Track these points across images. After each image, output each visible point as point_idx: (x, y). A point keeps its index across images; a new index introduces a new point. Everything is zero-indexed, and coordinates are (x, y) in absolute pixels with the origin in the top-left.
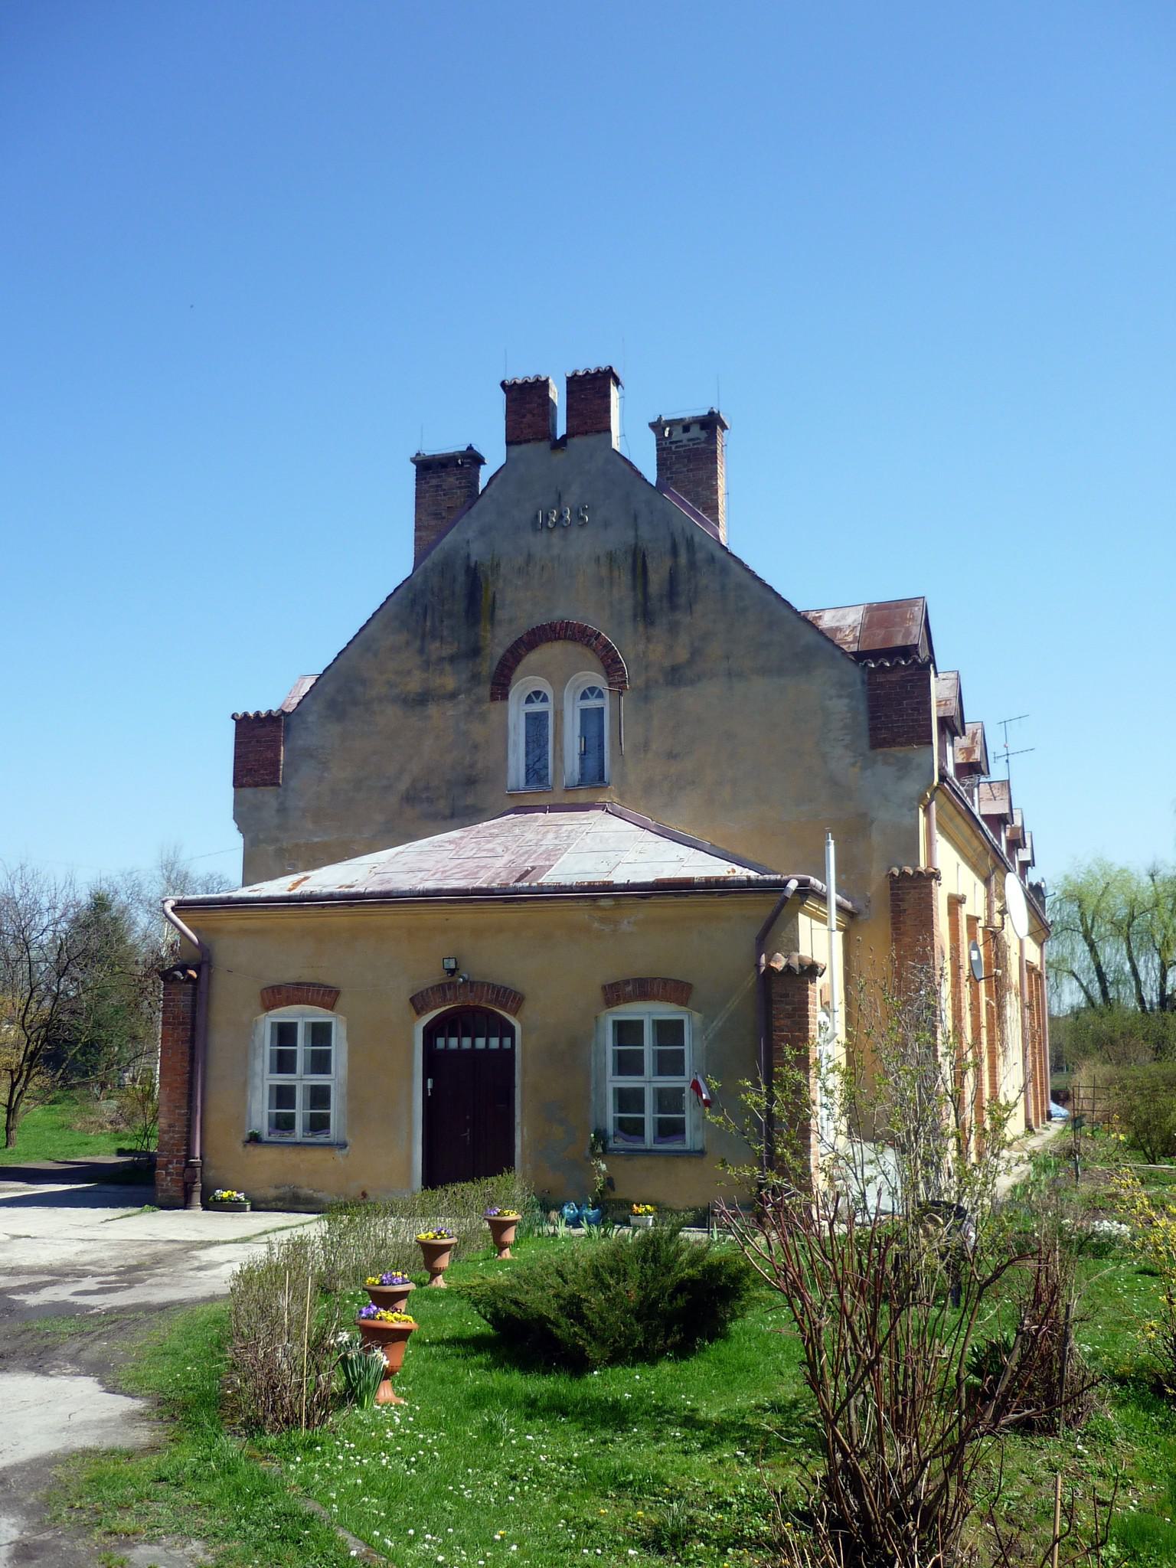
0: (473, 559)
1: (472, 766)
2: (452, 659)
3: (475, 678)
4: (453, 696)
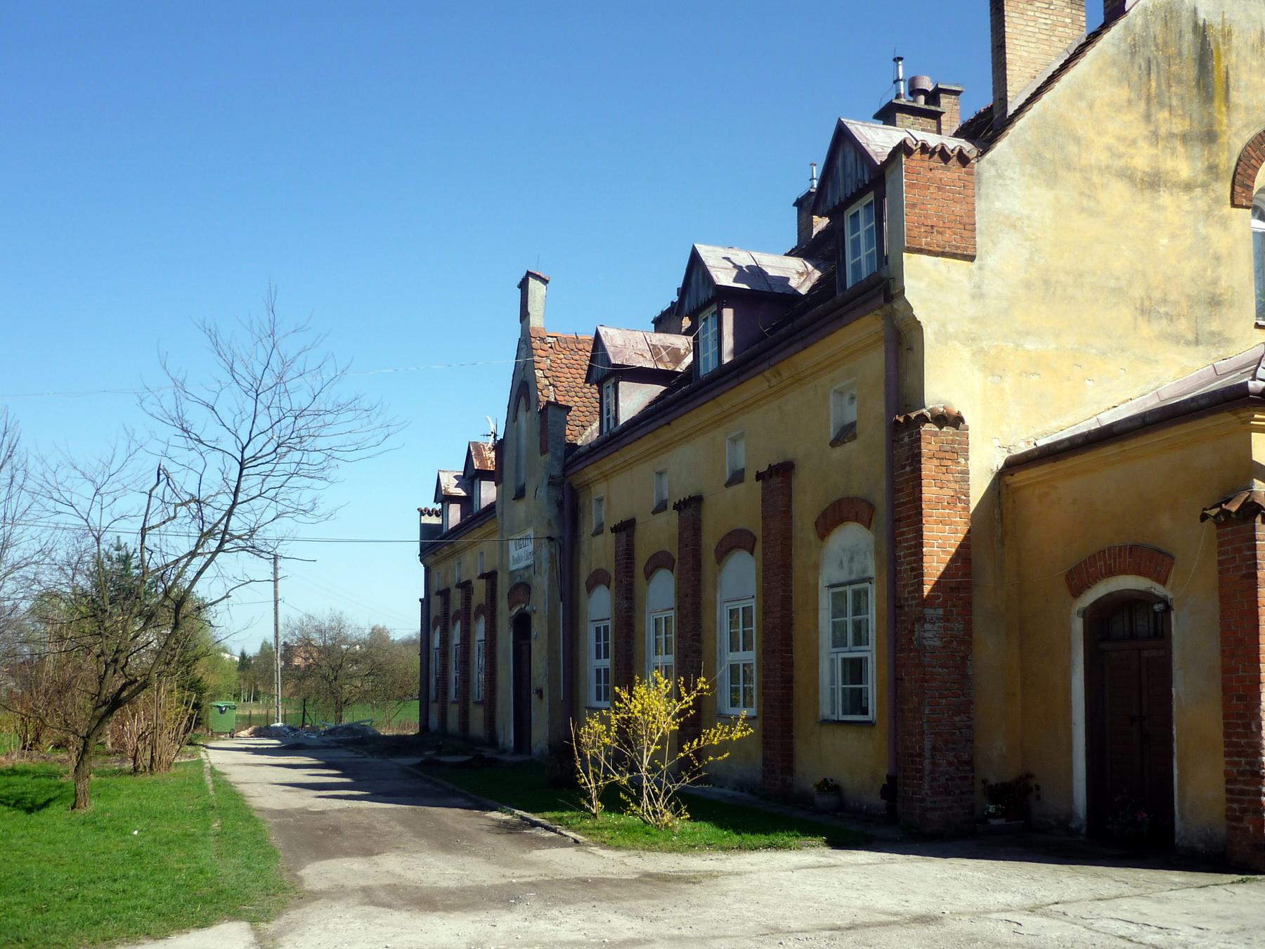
0: (1202, 16)
1: (1215, 282)
2: (1185, 138)
3: (1212, 169)
4: (1188, 187)
